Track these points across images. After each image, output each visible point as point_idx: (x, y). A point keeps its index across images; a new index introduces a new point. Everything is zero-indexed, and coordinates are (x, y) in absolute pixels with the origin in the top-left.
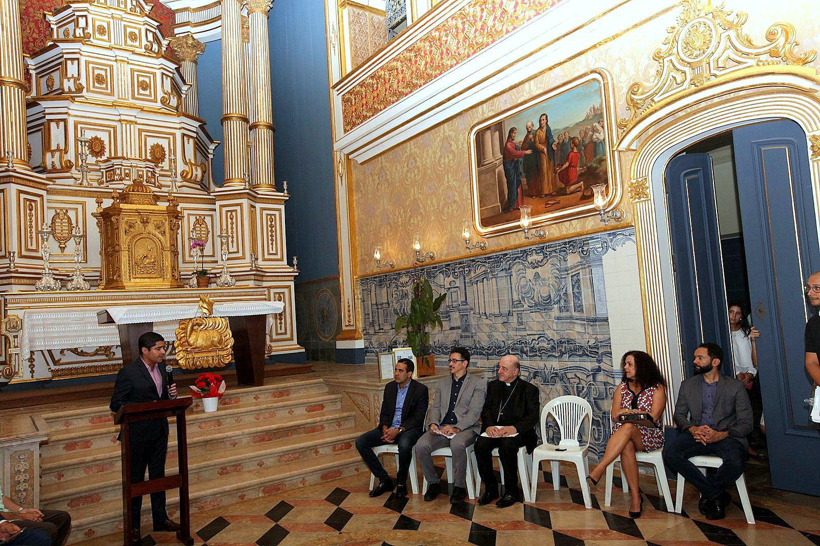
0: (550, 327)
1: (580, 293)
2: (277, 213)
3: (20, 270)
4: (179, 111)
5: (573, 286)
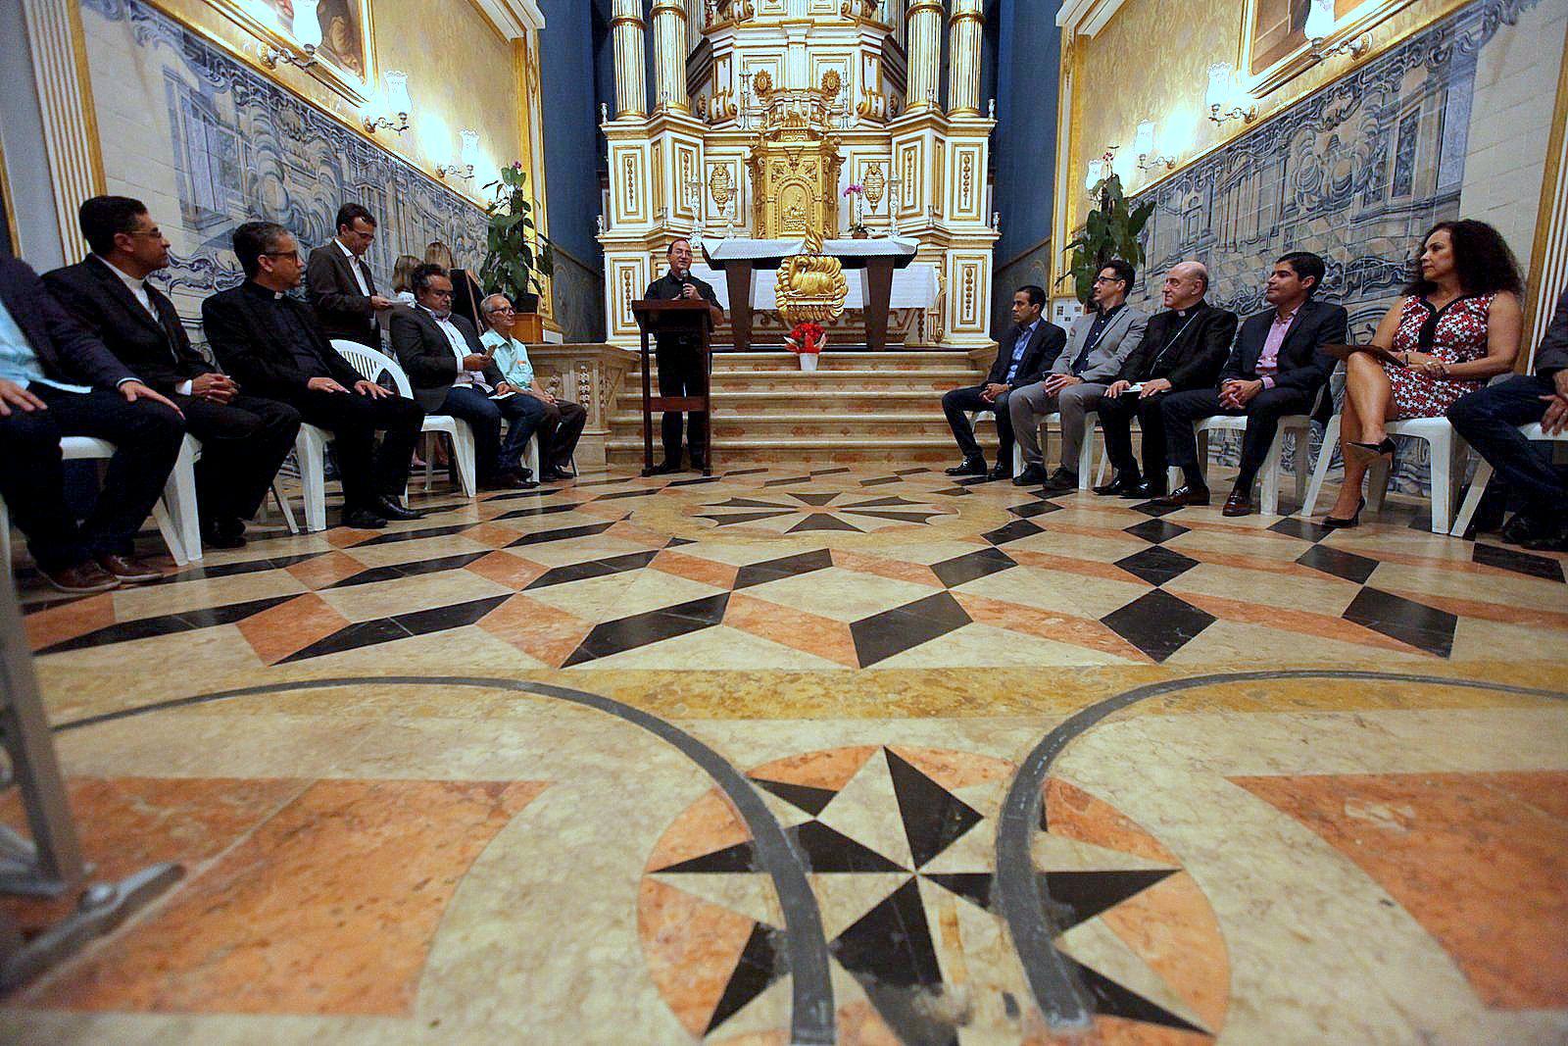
0: (1339, 241)
1: (1411, 154)
2: (976, 150)
3: (672, 229)
4: (866, 20)
5: (1401, 142)
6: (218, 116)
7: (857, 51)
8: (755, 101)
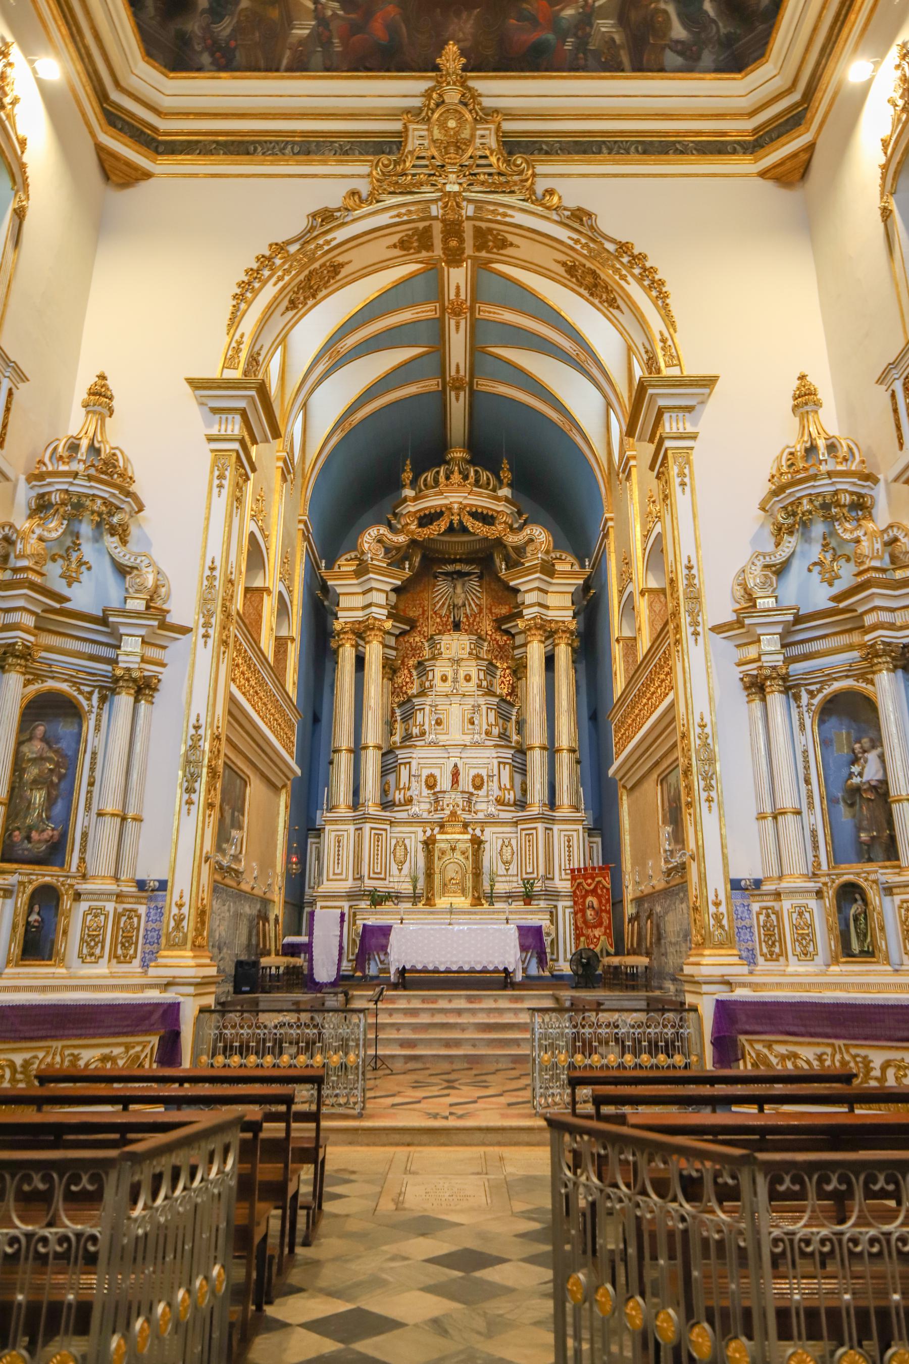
2: (575, 833)
7: (495, 762)
8: (426, 792)
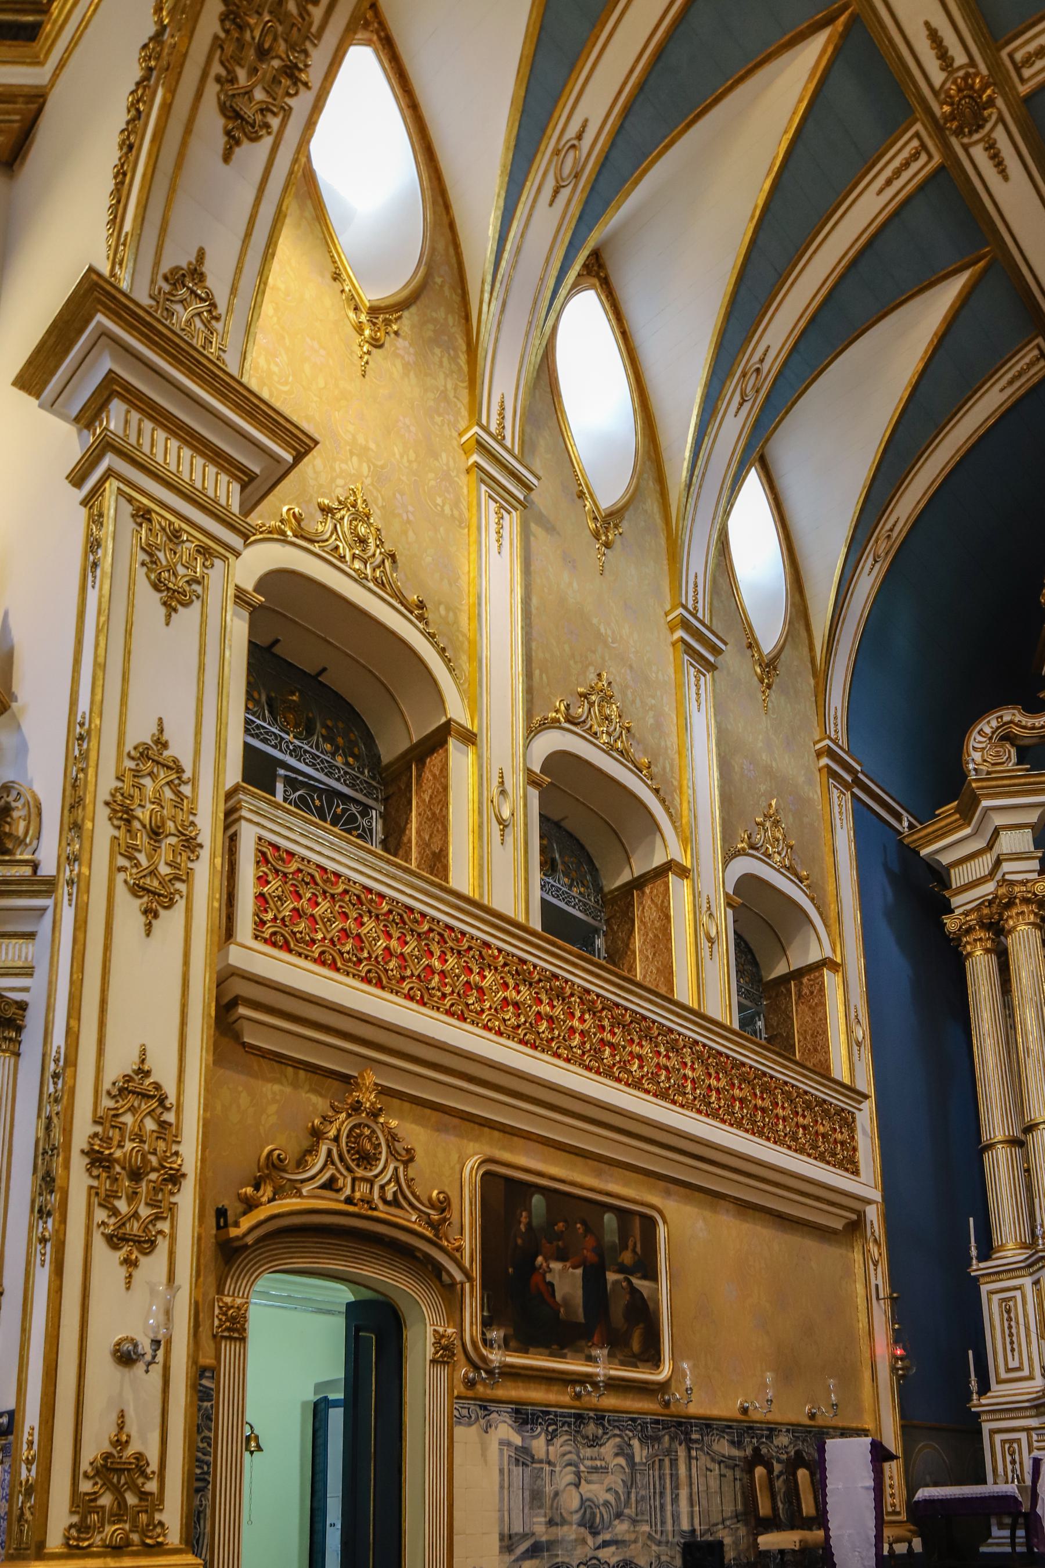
6: (533, 1457)
